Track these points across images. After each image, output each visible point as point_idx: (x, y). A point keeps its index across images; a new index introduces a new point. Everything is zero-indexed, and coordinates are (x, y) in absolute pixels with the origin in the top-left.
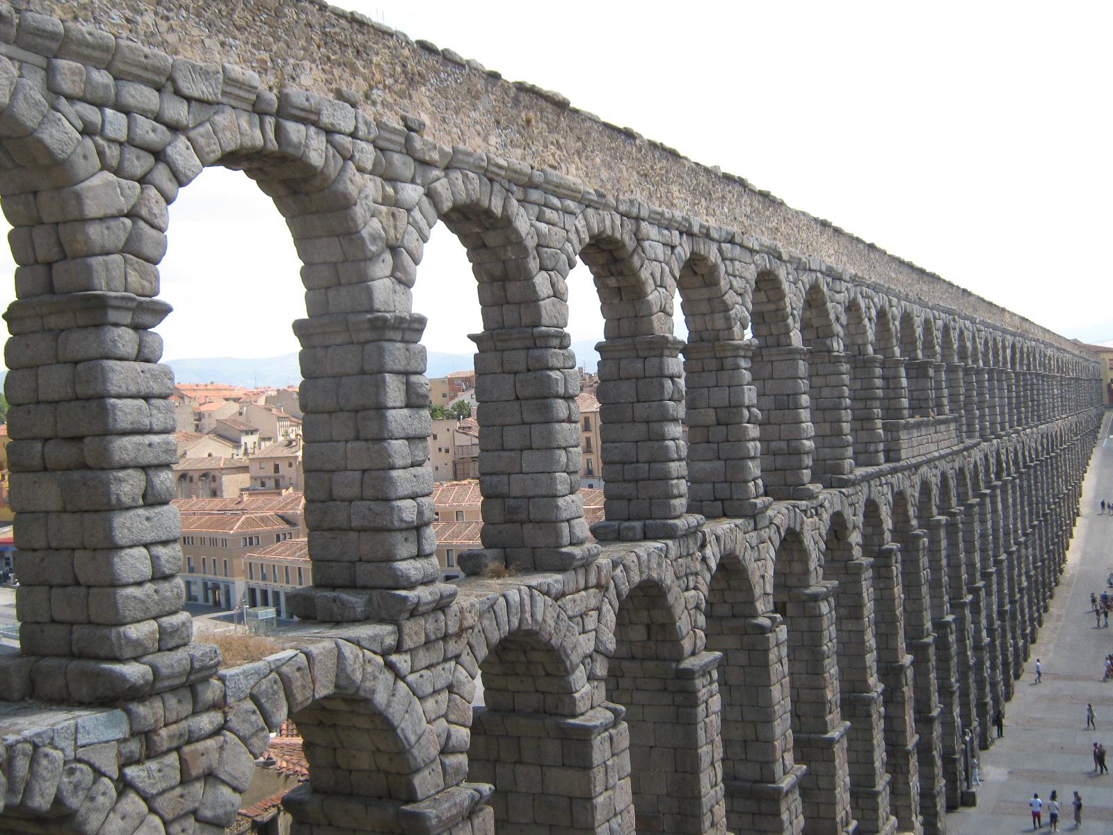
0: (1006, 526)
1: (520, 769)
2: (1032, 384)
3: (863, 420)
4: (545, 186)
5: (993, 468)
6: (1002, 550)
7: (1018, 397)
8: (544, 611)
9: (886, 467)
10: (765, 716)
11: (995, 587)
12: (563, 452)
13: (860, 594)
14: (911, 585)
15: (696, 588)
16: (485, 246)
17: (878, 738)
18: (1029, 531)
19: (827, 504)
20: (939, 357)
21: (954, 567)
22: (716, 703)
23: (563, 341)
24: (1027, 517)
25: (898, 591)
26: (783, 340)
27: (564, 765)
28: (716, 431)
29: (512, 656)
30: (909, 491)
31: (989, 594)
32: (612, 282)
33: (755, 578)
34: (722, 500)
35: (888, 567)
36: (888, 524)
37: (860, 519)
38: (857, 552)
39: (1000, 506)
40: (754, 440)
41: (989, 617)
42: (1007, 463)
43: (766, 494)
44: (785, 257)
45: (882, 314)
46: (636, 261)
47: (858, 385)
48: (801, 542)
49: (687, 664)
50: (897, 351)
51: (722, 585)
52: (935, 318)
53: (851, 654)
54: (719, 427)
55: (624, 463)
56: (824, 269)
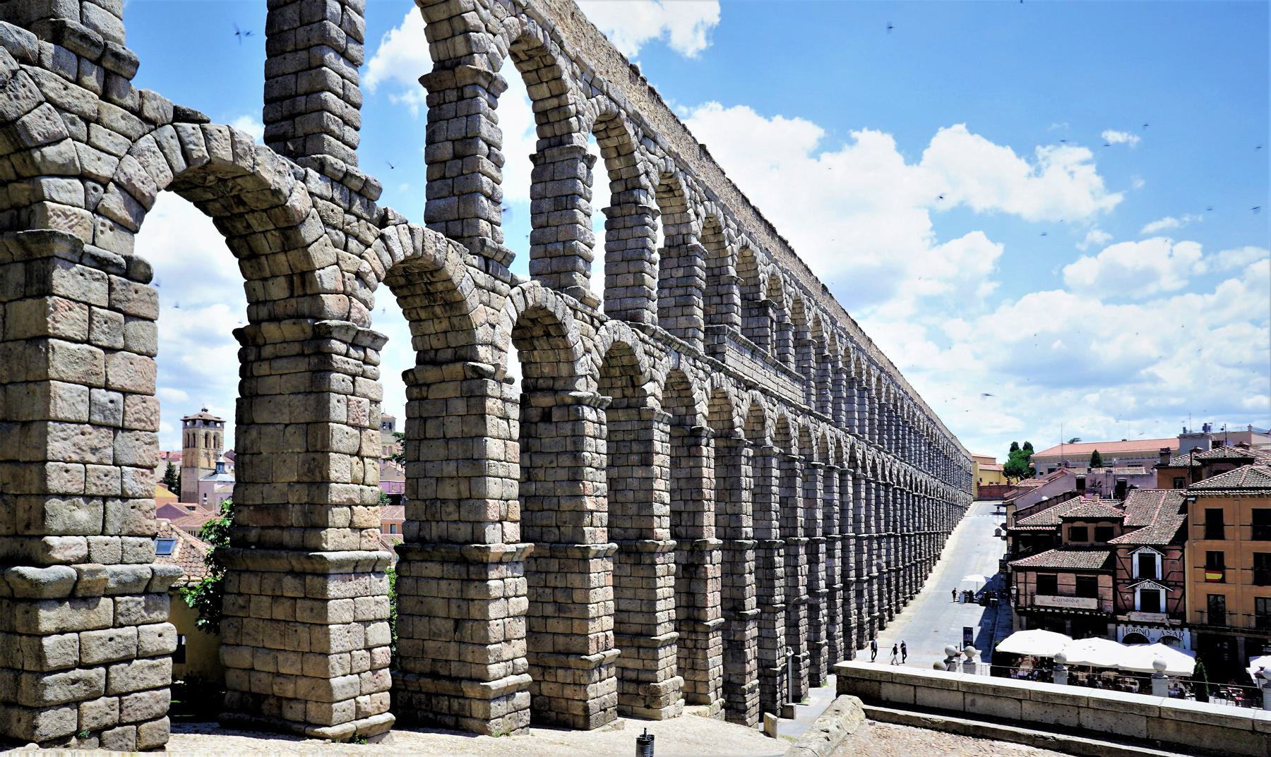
6: (850, 529)
7: (881, 422)
10: (476, 465)
11: (838, 553)
13: (650, 441)
24: (882, 523)
26: (565, 138)
30: (734, 400)
31: (830, 554)
33: (479, 315)
35: (698, 445)
37: (661, 376)
39: (850, 490)
47: (680, 273)
48: (564, 336)
50: (733, 272)
51: (445, 325)
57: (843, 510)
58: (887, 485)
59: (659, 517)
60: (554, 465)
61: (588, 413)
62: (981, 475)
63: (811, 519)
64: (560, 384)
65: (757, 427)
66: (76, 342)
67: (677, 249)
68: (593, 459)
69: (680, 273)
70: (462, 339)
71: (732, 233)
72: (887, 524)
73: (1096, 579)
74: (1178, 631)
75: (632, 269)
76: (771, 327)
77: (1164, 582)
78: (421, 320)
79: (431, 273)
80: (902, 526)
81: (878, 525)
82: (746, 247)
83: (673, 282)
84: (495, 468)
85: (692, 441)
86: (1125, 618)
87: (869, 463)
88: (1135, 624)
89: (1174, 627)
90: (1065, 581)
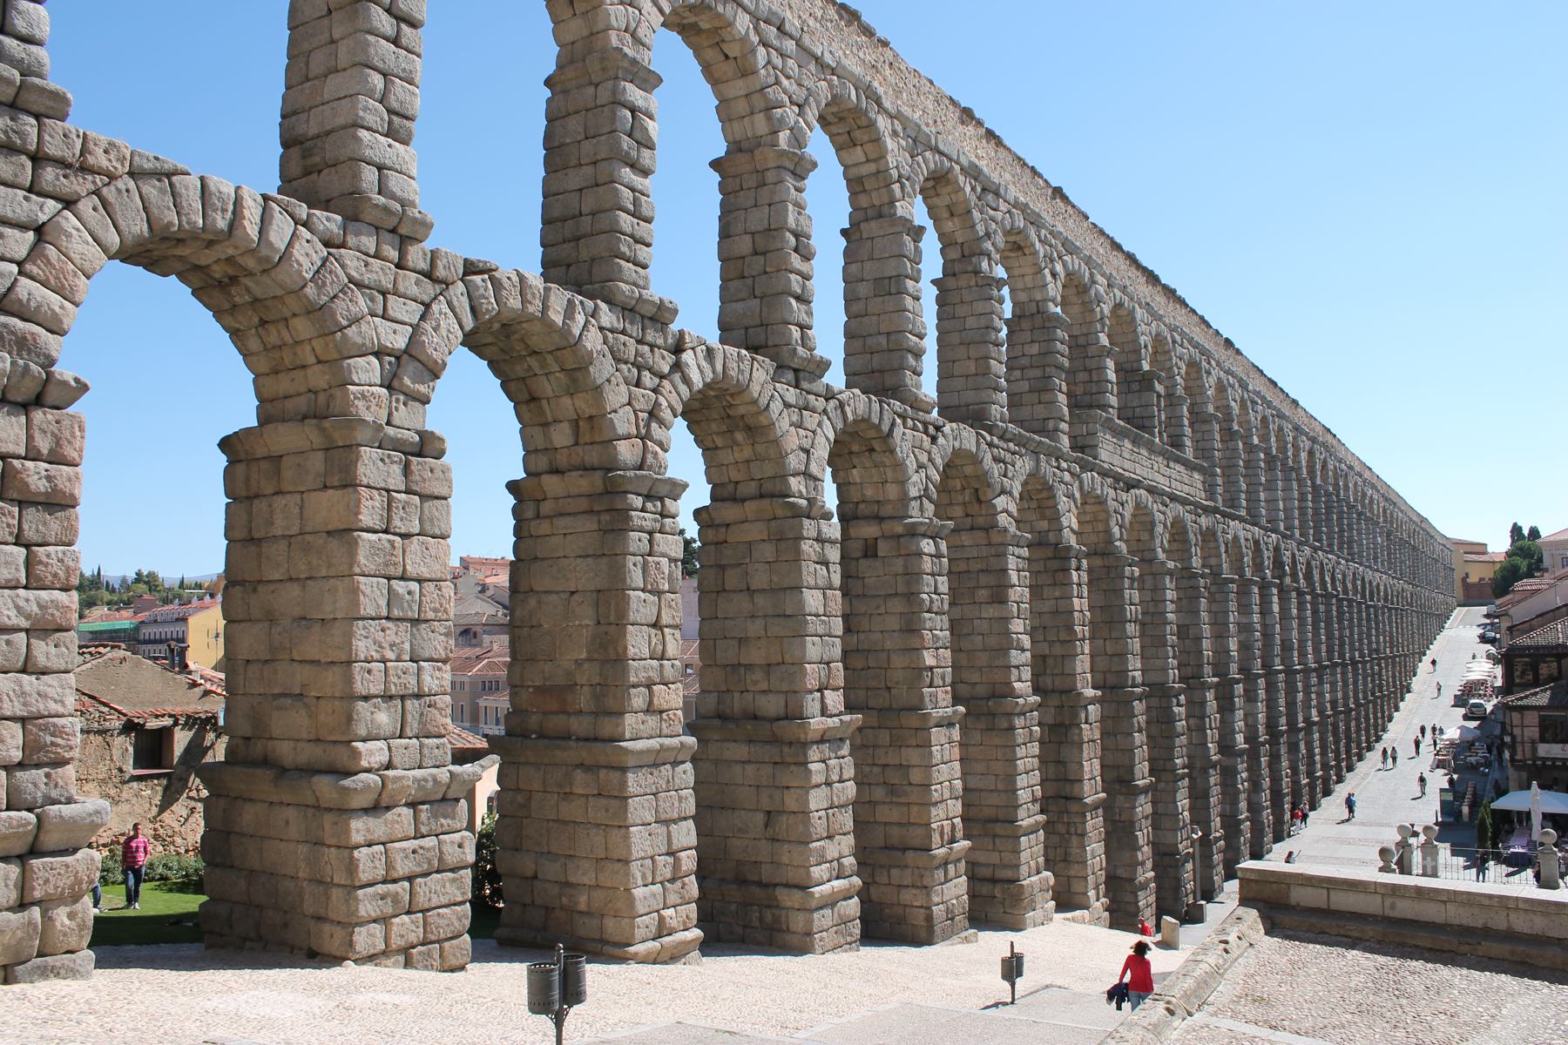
1: (280, 501)
6: (1277, 660)
10: (794, 623)
11: (1262, 694)
12: (377, 80)
13: (1004, 571)
15: (655, 391)
19: (947, 429)
20: (1180, 391)
30: (1112, 504)
31: (1250, 697)
39: (1276, 608)
44: (887, 104)
47: (1035, 349)
48: (892, 452)
50: (1104, 340)
51: (748, 452)
52: (1174, 342)
57: (1267, 636)
58: (1328, 596)
59: (1017, 667)
60: (882, 610)
61: (927, 546)
63: (1222, 652)
64: (887, 510)
65: (1145, 536)
66: (375, 532)
67: (1030, 318)
68: (932, 601)
69: (1035, 349)
71: (1101, 290)
72: (1330, 651)
75: (973, 354)
76: (1158, 405)
78: (717, 448)
79: (732, 395)
80: (1352, 650)
81: (1316, 650)
82: (1119, 306)
83: (1025, 361)
84: (814, 625)
85: (1055, 564)
87: (1302, 568)
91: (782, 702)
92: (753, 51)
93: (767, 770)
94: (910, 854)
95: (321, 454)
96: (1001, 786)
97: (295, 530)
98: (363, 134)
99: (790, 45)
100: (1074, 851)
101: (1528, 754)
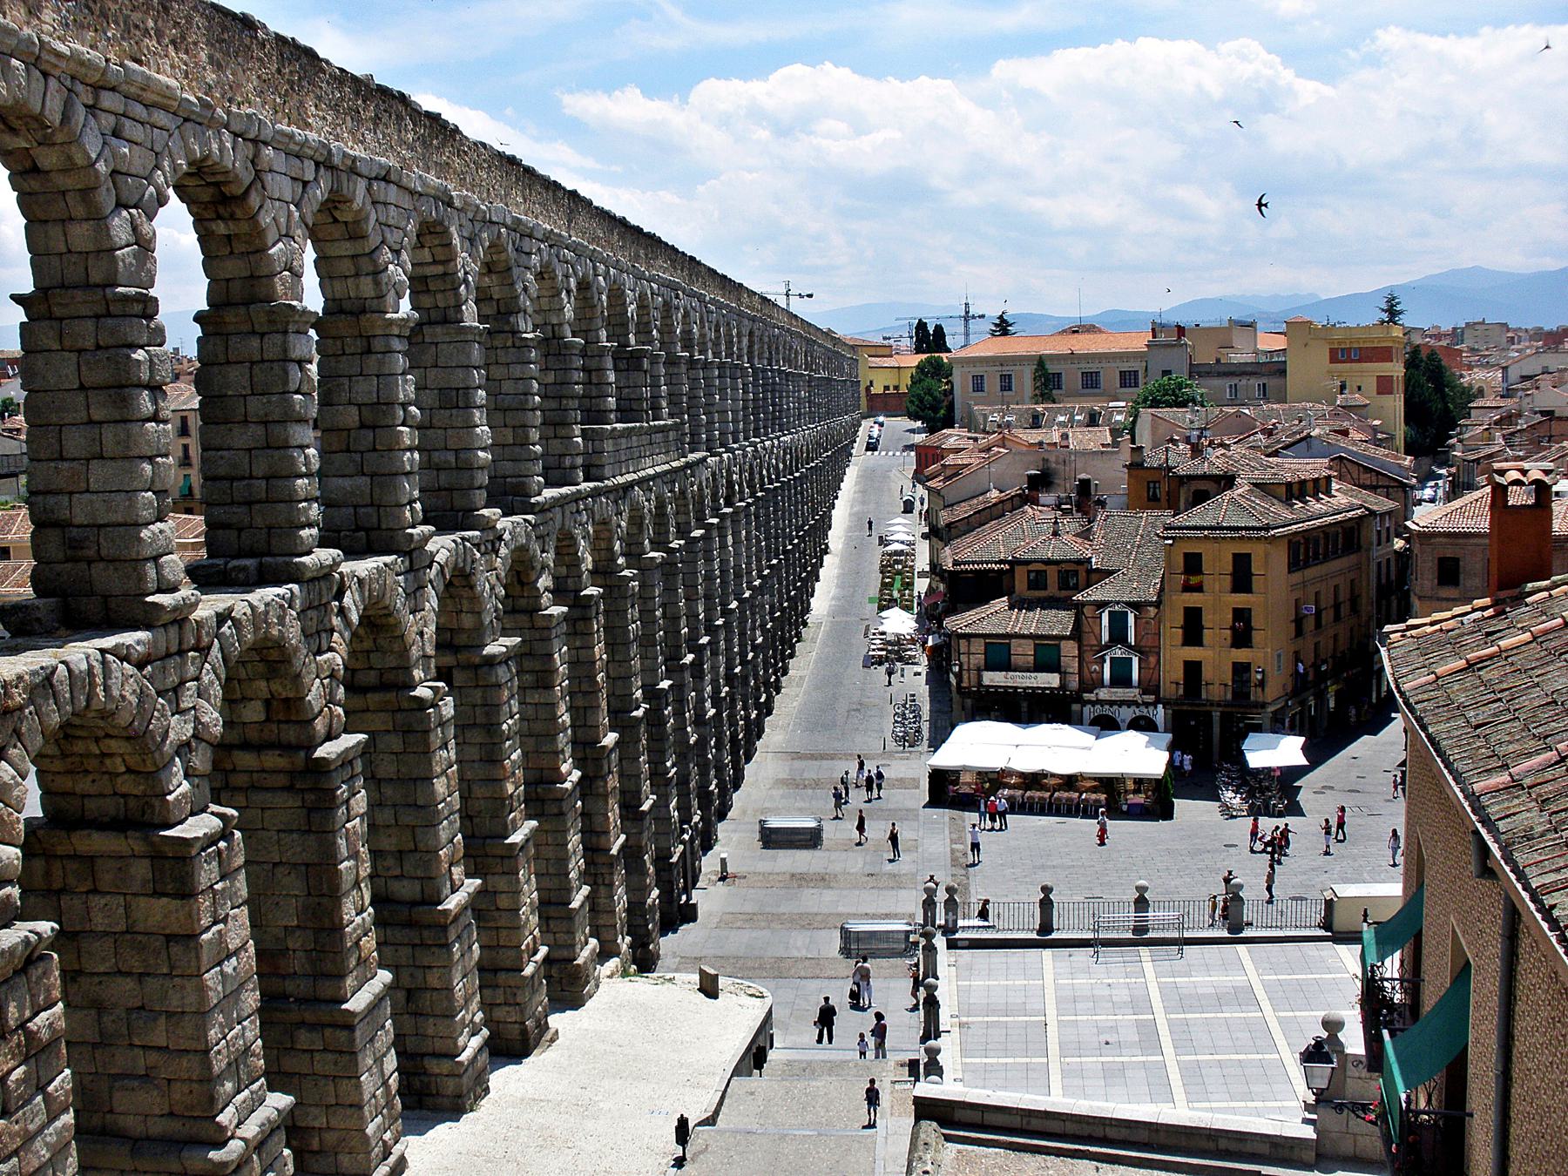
0: (737, 566)
1: (97, 901)
2: (774, 383)
3: (555, 425)
4: (124, 87)
5: (722, 491)
8: (126, 683)
9: (586, 486)
10: (428, 815)
12: (148, 468)
14: (616, 643)
15: (331, 649)
16: (35, 170)
17: (574, 841)
18: (766, 572)
19: (507, 536)
21: (672, 619)
22: (360, 802)
23: (149, 307)
25: (599, 650)
27: (157, 894)
28: (357, 440)
29: (79, 747)
31: (715, 653)
32: (221, 228)
33: (412, 635)
34: (367, 530)
36: (588, 563)
37: (549, 557)
38: (546, 598)
40: (410, 449)
41: (714, 682)
42: (741, 485)
43: (425, 522)
44: (457, 203)
45: (584, 286)
46: (254, 200)
47: (550, 378)
48: (472, 587)
49: (323, 751)
50: (603, 334)
51: (368, 644)
53: (538, 735)
54: (363, 432)
55: (233, 479)
56: (509, 221)
62: (872, 375)
70: (391, 661)
73: (1058, 646)
74: (1151, 708)
77: (1136, 649)
81: (759, 561)
86: (1092, 697)
88: (1102, 702)
89: (1147, 705)
90: (1020, 651)
91: (418, 888)
92: (367, 218)
93: (405, 952)
94: (502, 977)
95: (146, 863)
96: (551, 871)
97: (122, 927)
98: (145, 533)
99: (392, 193)
100: (602, 901)
101: (974, 681)
